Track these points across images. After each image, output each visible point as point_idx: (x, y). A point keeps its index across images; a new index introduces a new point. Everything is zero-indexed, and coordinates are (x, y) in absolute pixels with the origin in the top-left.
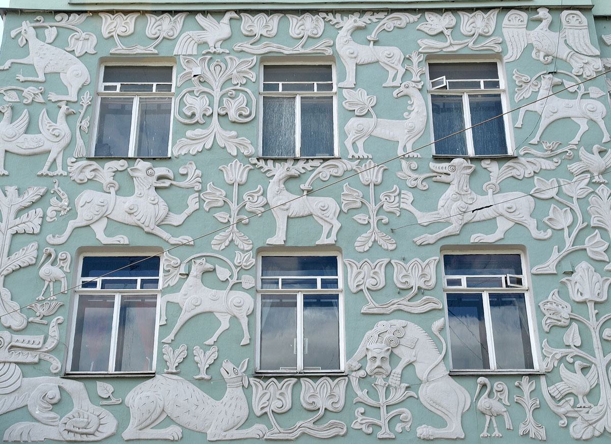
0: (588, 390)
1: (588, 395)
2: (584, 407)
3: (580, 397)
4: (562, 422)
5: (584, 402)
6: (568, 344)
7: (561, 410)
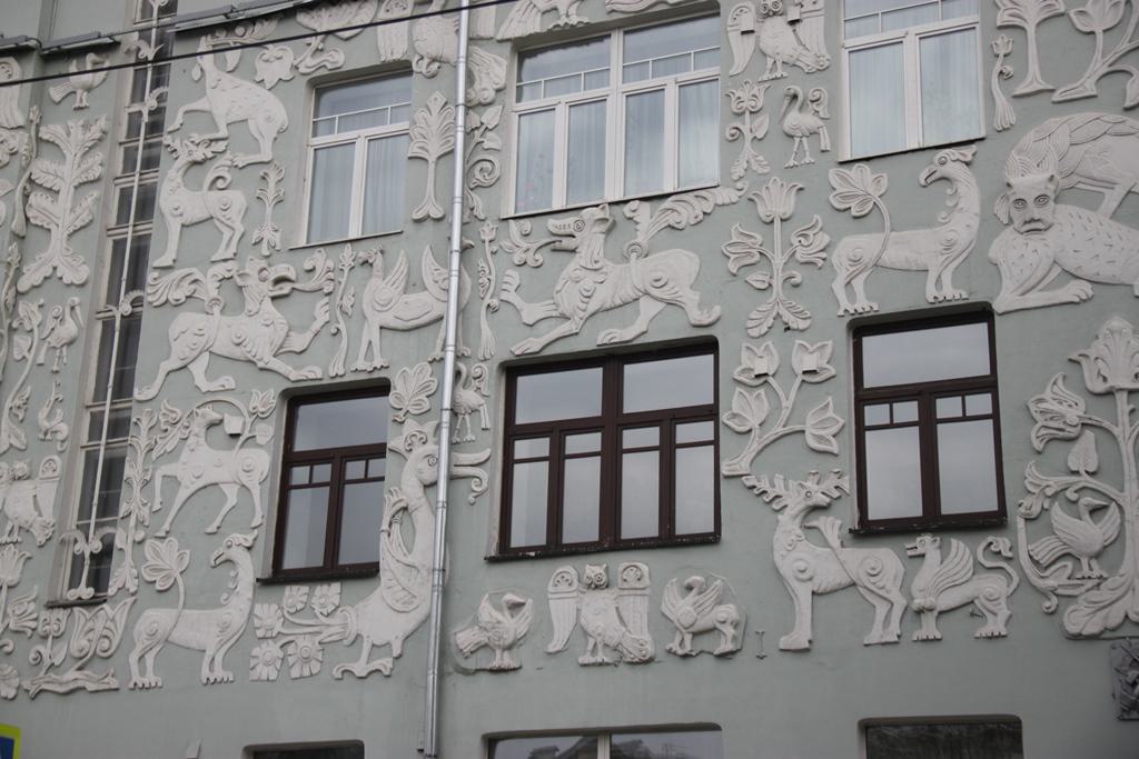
0: (1097, 547)
1: (1097, 556)
2: (1089, 578)
3: (1084, 561)
4: (1047, 604)
5: (1091, 569)
6: (1074, 469)
7: (1051, 582)
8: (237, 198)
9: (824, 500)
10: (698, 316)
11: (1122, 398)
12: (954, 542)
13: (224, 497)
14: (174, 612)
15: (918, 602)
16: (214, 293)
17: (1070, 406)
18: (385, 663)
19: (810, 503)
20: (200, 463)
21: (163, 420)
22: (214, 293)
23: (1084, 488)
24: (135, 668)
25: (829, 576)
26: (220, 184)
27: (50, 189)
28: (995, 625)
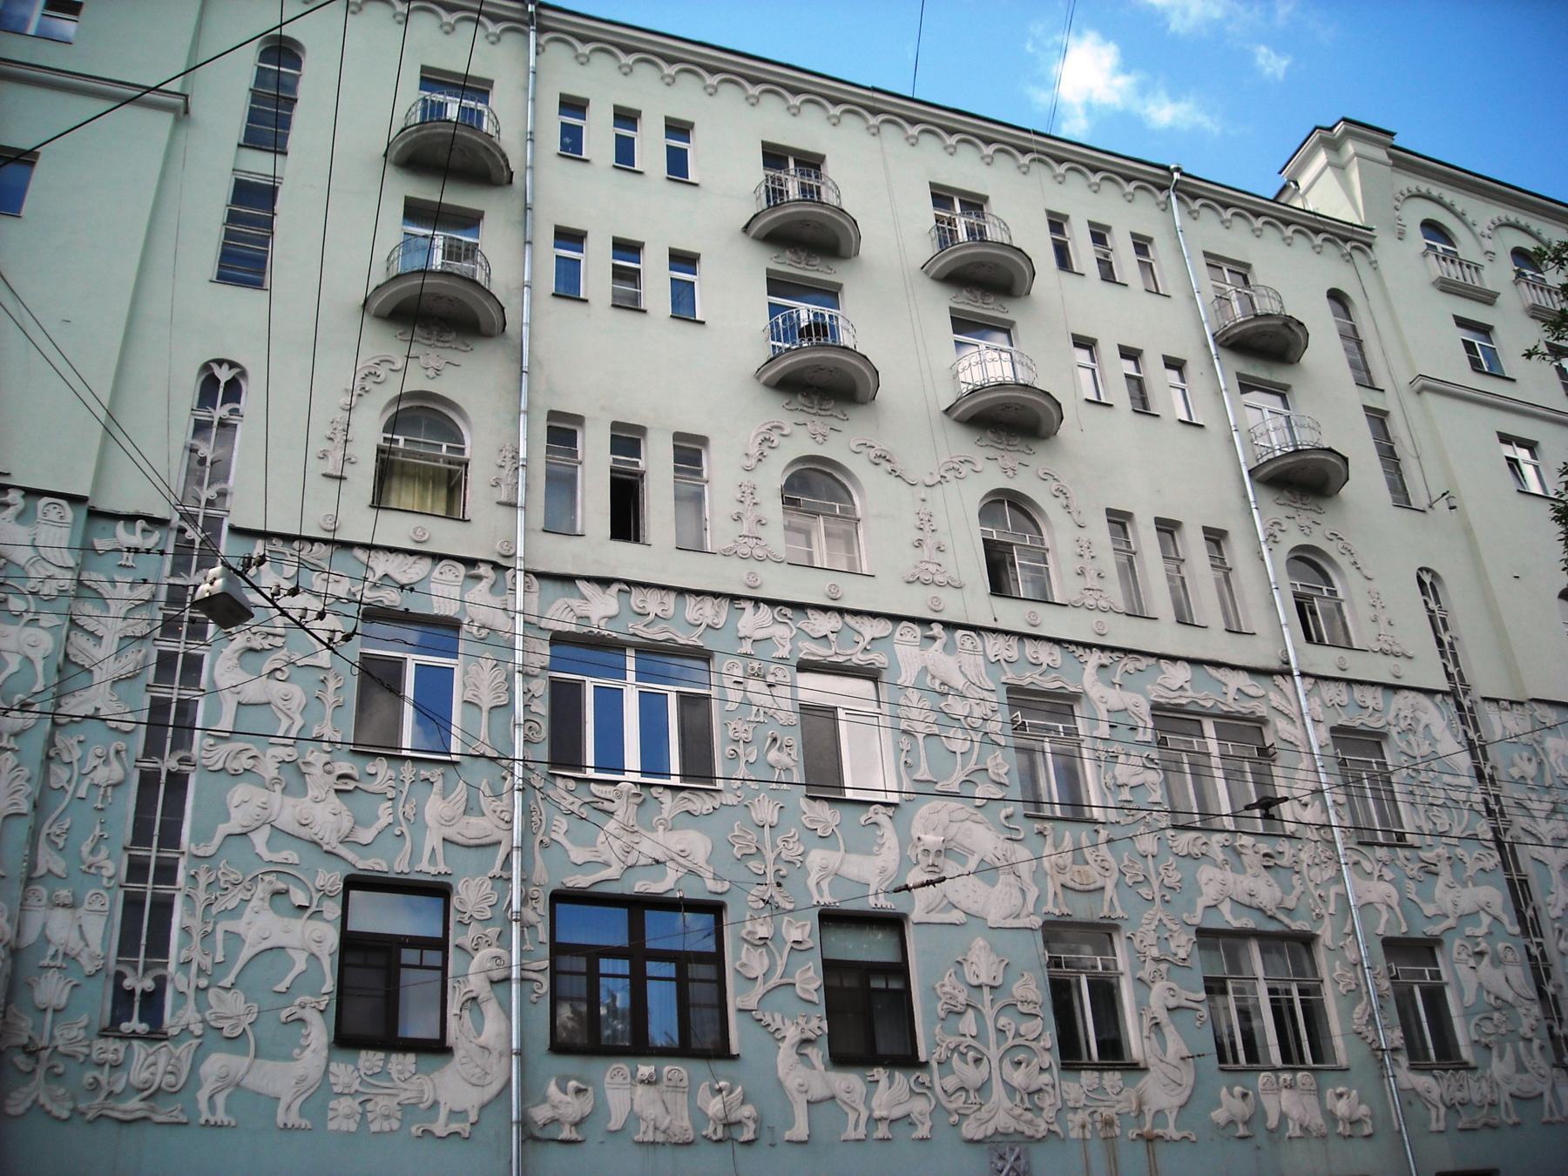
1: (978, 1090)
3: (972, 1093)
8: (297, 693)
9: (812, 1036)
10: (712, 885)
11: (986, 990)
12: (897, 1074)
13: (292, 963)
14: (246, 1061)
15: (877, 1114)
16: (275, 773)
18: (463, 1127)
19: (804, 1036)
20: (261, 925)
21: (223, 879)
22: (275, 773)
24: (203, 1105)
25: (818, 1091)
26: (278, 674)
27: (92, 633)
28: (923, 1131)
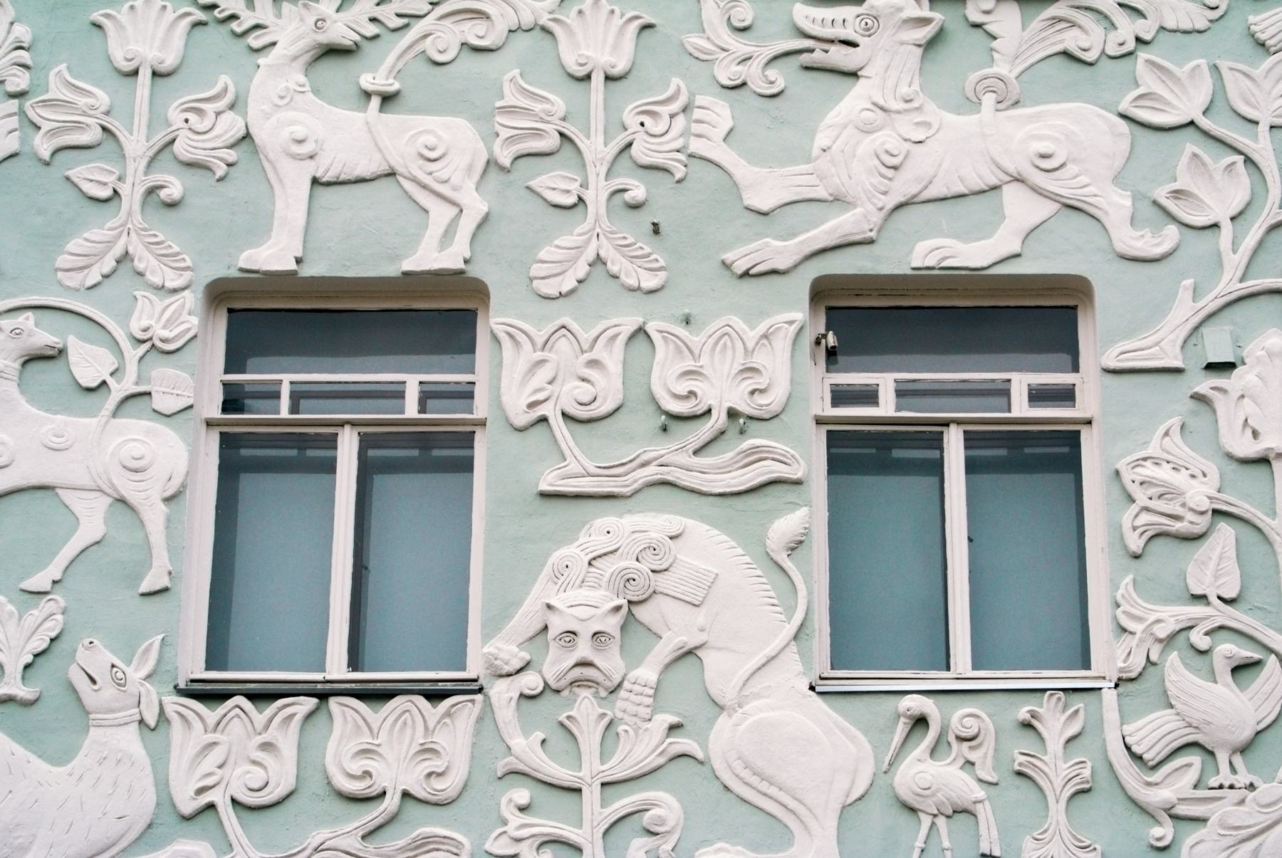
0: (1246, 734)
1: (1244, 749)
2: (1231, 787)
3: (1222, 757)
5: (1234, 770)
17: (1193, 476)
23: (1221, 628)
